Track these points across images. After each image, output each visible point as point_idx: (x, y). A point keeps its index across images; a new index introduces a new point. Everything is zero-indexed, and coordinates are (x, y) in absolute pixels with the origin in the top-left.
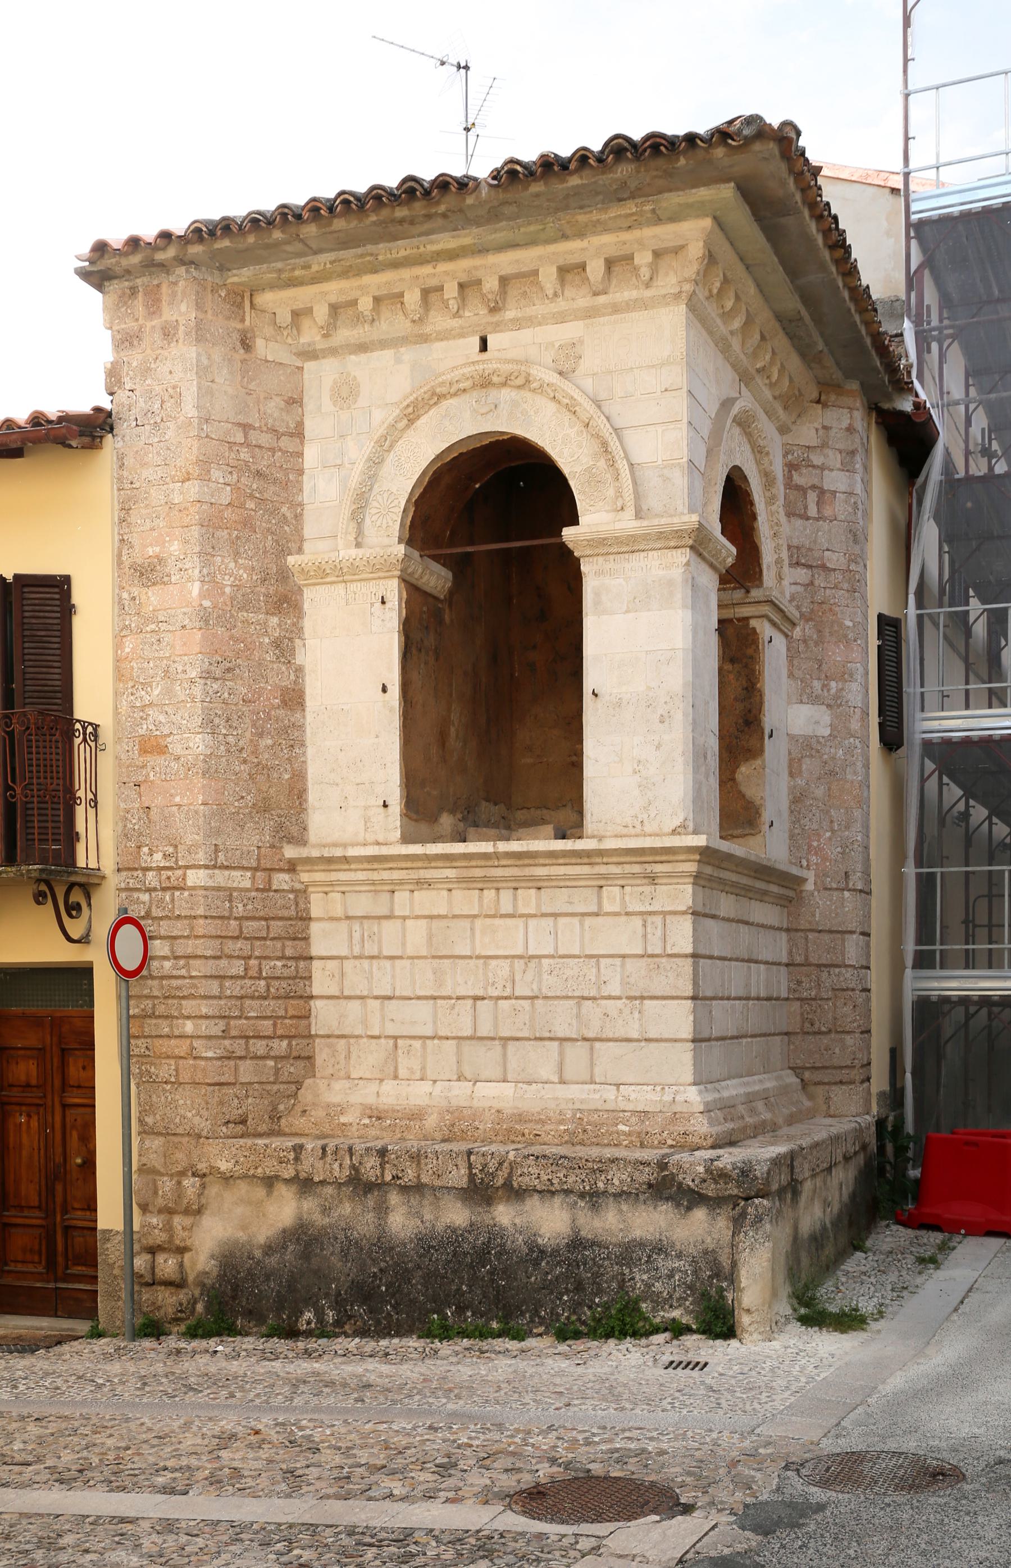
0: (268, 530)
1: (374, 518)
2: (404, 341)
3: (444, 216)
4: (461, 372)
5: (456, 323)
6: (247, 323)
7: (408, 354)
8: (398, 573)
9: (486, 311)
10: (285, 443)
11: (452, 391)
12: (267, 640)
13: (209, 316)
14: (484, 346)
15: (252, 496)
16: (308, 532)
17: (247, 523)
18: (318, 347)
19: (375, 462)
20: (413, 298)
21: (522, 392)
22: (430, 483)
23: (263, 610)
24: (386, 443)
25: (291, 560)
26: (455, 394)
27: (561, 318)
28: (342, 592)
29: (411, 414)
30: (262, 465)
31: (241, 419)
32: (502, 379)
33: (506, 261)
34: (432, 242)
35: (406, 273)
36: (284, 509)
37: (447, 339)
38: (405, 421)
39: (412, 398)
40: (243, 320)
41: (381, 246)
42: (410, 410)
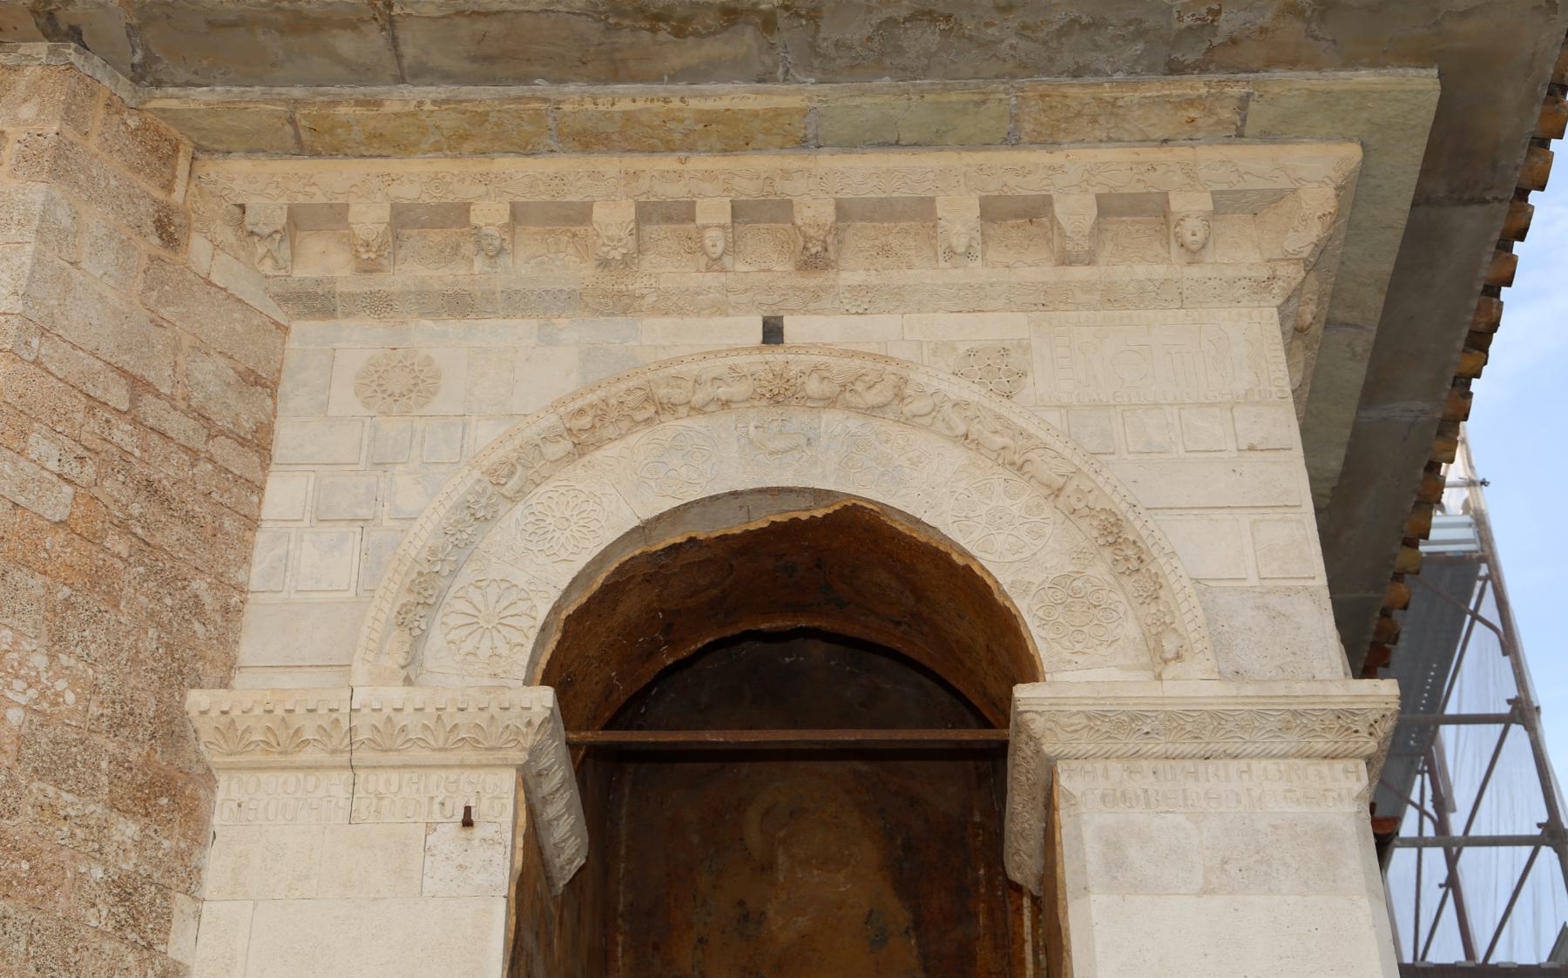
0: (152, 615)
1: (453, 635)
2: (575, 301)
3: (768, 23)
4: (731, 360)
5: (712, 280)
6: (177, 197)
7: (575, 332)
8: (520, 757)
9: (789, 267)
10: (223, 449)
11: (698, 399)
12: (98, 873)
13: (93, 143)
14: (773, 333)
15: (123, 527)
16: (249, 649)
17: (98, 578)
18: (339, 289)
19: (477, 515)
20: (613, 218)
22: (606, 589)
23: (104, 794)
24: (508, 480)
25: (197, 700)
26: (699, 410)
27: (972, 301)
28: (340, 793)
29: (585, 431)
30: (164, 474)
31: (128, 361)
32: (828, 389)
33: (866, 173)
34: (702, 96)
35: (610, 165)
36: (200, 585)
37: (681, 312)
38: (566, 445)
39: (593, 398)
40: (168, 187)
41: (571, 87)
42: (585, 421)
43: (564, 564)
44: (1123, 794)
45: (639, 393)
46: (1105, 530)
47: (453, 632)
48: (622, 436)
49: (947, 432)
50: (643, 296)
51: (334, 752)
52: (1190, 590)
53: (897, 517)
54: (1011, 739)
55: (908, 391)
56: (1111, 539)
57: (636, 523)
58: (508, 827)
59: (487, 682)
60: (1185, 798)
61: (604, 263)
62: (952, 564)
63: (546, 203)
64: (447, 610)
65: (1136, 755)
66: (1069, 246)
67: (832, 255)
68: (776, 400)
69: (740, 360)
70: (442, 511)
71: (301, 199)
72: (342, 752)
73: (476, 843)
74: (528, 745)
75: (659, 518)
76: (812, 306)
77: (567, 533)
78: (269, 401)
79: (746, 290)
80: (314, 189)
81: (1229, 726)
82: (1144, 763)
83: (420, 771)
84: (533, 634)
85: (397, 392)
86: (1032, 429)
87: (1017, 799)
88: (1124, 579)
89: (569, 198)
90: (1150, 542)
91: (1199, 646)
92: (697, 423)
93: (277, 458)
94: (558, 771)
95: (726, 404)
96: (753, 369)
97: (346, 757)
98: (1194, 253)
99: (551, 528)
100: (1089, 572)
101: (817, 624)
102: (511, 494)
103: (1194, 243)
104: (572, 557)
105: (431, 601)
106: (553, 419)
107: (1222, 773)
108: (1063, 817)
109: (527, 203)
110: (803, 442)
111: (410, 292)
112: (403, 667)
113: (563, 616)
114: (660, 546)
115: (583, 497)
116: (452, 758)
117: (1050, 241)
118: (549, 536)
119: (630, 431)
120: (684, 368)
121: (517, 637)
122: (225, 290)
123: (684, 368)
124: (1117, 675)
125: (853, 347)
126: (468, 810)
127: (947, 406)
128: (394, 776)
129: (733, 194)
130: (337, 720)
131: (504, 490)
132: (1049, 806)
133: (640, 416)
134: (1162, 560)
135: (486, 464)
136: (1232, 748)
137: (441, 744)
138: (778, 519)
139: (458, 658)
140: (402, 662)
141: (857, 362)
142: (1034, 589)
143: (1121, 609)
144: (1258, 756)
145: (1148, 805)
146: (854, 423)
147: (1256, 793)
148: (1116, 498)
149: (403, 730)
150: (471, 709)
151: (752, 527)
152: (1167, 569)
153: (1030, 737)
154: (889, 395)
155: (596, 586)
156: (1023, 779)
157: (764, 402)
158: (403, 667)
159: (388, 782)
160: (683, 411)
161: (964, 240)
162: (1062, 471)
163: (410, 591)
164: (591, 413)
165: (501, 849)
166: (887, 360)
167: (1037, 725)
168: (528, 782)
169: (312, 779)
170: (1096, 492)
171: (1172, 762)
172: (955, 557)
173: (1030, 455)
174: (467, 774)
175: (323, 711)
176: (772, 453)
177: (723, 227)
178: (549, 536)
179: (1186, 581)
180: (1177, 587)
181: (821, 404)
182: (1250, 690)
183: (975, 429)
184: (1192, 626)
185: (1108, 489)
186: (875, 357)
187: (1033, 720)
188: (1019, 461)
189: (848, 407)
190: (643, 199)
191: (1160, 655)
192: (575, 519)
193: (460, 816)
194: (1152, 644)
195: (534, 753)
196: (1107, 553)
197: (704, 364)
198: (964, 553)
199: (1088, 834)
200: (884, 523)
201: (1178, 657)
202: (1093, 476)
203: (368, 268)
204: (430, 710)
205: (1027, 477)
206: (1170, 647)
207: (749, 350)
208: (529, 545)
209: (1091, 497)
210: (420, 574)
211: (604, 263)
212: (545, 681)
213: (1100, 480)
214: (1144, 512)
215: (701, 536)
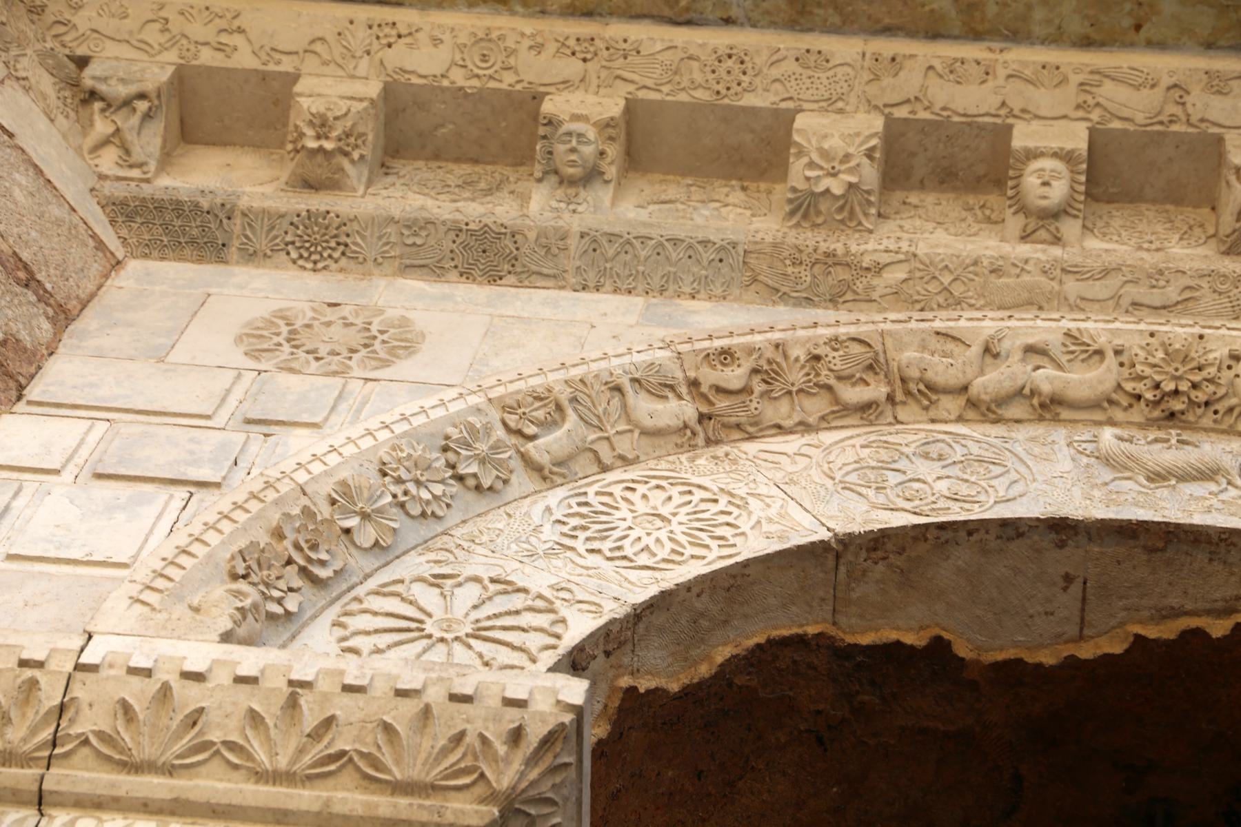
11: (991, 381)
26: (986, 410)
38: (684, 409)
42: (734, 376)
45: (856, 349)
48: (805, 427)
50: (879, 269)
63: (696, 108)
71: (207, 57)
72: (26, 760)
78: (46, 325)
79: (1106, 272)
80: (237, 40)
89: (750, 100)
93: (34, 391)
96: (1118, 342)
102: (544, 460)
109: (662, 102)
114: (866, 640)
118: (616, 534)
119: (825, 423)
122: (11, 135)
129: (1095, 115)
137: (283, 762)
138: (1152, 632)
151: (1086, 652)
155: (704, 670)
157: (1138, 414)
177: (1067, 157)
178: (616, 534)
190: (902, 113)
211: (805, 208)
215: (962, 650)
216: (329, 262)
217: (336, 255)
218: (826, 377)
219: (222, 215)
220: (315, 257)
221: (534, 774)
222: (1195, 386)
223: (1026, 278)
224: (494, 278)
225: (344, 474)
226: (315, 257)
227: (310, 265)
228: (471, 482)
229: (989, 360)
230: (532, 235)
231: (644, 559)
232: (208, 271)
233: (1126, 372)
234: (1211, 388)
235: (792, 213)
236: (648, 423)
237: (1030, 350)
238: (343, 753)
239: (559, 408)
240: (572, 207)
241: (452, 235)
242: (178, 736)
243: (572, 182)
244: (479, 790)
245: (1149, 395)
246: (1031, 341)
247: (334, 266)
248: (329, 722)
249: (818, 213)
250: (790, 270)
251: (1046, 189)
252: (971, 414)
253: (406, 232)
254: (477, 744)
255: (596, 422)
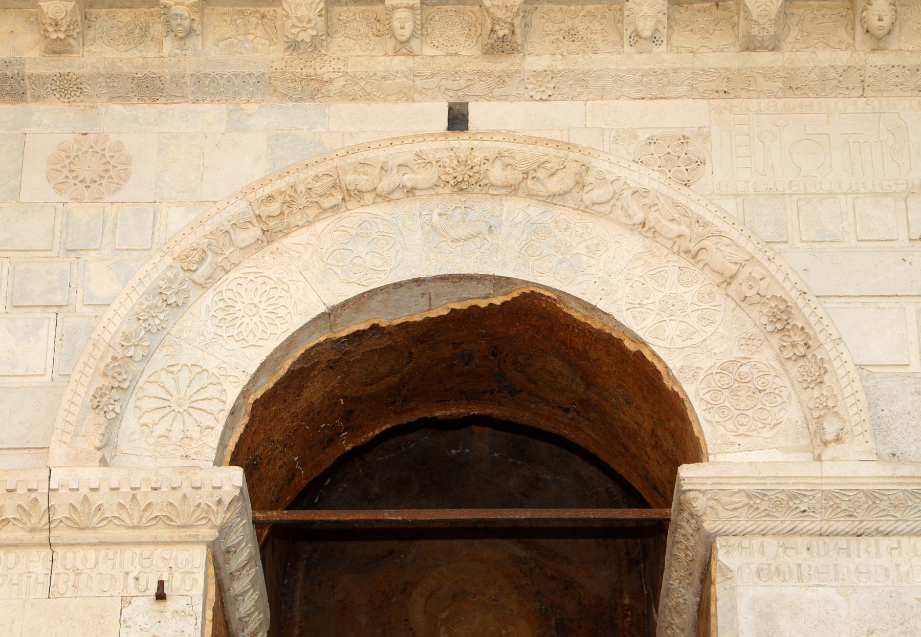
2: (263, 85)
4: (417, 147)
5: (399, 64)
7: (264, 116)
8: (211, 534)
9: (476, 51)
11: (384, 185)
14: (458, 120)
18: (28, 71)
19: (169, 301)
21: (556, 211)
22: (292, 374)
24: (199, 267)
26: (385, 197)
27: (656, 88)
28: (40, 569)
32: (512, 176)
37: (368, 97)
38: (255, 232)
39: (281, 184)
42: (274, 208)
43: (252, 350)
44: (777, 569)
45: (327, 180)
46: (774, 317)
47: (147, 416)
48: (309, 223)
49: (626, 220)
50: (331, 81)
51: (33, 530)
52: (854, 375)
53: (573, 304)
54: (672, 517)
55: (589, 179)
56: (779, 326)
57: (323, 309)
58: (199, 600)
59: (179, 463)
60: (836, 573)
61: (293, 46)
62: (623, 350)
64: (140, 394)
65: (792, 532)
66: (755, 31)
67: (519, 39)
68: (459, 187)
69: (426, 147)
70: (135, 297)
72: (41, 530)
73: (169, 615)
74: (218, 522)
75: (344, 305)
76: (497, 92)
77: (256, 319)
79: (433, 75)
81: (883, 505)
82: (799, 540)
83: (117, 549)
84: (223, 417)
85: (88, 180)
86: (709, 217)
87: (674, 575)
88: (790, 365)
90: (817, 328)
91: (859, 429)
92: (382, 210)
94: (245, 549)
95: (411, 191)
96: (438, 156)
97: (45, 534)
98: (879, 39)
99: (240, 314)
100: (756, 357)
101: (489, 411)
102: (201, 281)
103: (881, 28)
104: (260, 343)
105: (125, 385)
106: (243, 205)
107: (873, 549)
108: (719, 590)
110: (485, 229)
111: (100, 75)
112: (99, 449)
113: (251, 400)
115: (271, 284)
116: (146, 535)
117: (735, 26)
118: (238, 322)
120: (371, 154)
121: (207, 421)
123: (371, 154)
124: (777, 456)
125: (537, 134)
126: (161, 584)
127: (627, 193)
128: (91, 553)
130: (36, 500)
131: (195, 276)
132: (706, 580)
133: (327, 203)
134: (828, 346)
135: (177, 250)
136: (884, 526)
139: (151, 440)
140: (98, 444)
141: (540, 149)
142: (702, 374)
143: (785, 394)
144: (910, 534)
145: (800, 579)
146: (535, 211)
147: (904, 568)
148: (787, 285)
149: (99, 509)
150: (164, 489)
152: (833, 355)
153: (692, 515)
154: (570, 182)
155: (282, 372)
156: (682, 555)
157: (448, 189)
158: (99, 449)
159: (85, 559)
160: (369, 198)
161: (650, 24)
162: (736, 259)
163: (105, 375)
164: (280, 199)
165: (192, 620)
166: (570, 147)
167: (700, 503)
168: (218, 558)
169: (12, 556)
170: (768, 280)
171: (826, 539)
172: (628, 344)
173: (705, 243)
174: (160, 551)
175: (22, 491)
176: (454, 241)
178: (238, 322)
179: (850, 367)
180: (841, 372)
181: (503, 191)
182: (906, 471)
183: (653, 217)
184: (854, 409)
185: (780, 277)
186: (558, 144)
187: (695, 499)
188: (694, 249)
189: (530, 195)
191: (820, 439)
192: (263, 306)
193: (153, 589)
194: (813, 427)
195: (224, 530)
196: (775, 340)
197: (391, 150)
198: (636, 339)
199: (742, 606)
200: (560, 310)
201: (838, 439)
202: (766, 263)
203: (57, 49)
204: (125, 489)
205: (701, 265)
206: (831, 428)
207: (435, 136)
208: (219, 331)
209: (763, 284)
210: (114, 358)
211: (293, 46)
212: (234, 462)
213: (772, 268)
214: (813, 299)
216: (75, 98)
217: (78, 94)
218: (314, 198)
219: (19, 79)
220: (68, 96)
221: (228, 516)
222: (470, 176)
223: (398, 80)
224: (155, 101)
225: (123, 329)
226: (68, 96)
227: (66, 100)
228: (174, 305)
229: (383, 172)
230: (168, 77)
231: (252, 340)
232: (18, 107)
233: (442, 169)
234: (478, 175)
235: (288, 48)
236: (242, 245)
237: (401, 165)
238: (157, 517)
239: (203, 251)
240: (183, 53)
241: (130, 80)
242: (94, 515)
243: (181, 39)
244: (210, 524)
245: (452, 183)
246: (401, 162)
247: (78, 100)
248: (149, 504)
249: (300, 48)
250: (291, 85)
251: (403, 31)
252: (378, 200)
253: (108, 80)
254: (206, 507)
255: (220, 252)
